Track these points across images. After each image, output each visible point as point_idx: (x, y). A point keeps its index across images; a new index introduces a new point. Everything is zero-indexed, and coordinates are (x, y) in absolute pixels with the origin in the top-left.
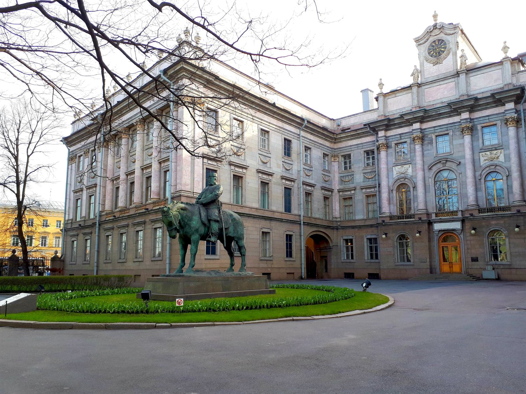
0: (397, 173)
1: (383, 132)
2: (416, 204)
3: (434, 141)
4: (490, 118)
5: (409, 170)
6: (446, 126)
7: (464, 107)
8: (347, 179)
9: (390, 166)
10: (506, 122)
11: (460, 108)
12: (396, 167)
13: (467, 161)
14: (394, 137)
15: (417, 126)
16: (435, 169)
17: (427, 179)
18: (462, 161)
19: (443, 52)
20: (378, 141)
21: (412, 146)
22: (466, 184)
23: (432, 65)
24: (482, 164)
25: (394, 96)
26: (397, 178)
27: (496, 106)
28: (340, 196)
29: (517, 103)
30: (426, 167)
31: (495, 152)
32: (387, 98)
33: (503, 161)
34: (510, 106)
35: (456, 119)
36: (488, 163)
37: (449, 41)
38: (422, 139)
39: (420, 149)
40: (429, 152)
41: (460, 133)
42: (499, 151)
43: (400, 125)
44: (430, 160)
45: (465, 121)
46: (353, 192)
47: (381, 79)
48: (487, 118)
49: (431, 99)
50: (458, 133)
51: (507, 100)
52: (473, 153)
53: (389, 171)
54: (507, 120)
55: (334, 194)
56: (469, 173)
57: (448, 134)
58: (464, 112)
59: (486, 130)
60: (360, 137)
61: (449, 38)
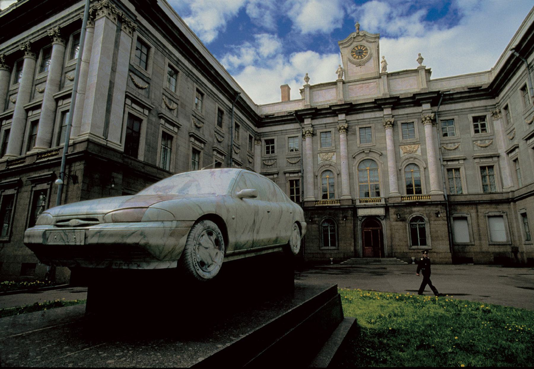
3: (358, 133)
15: (342, 117)
27: (414, 106)
30: (350, 155)
31: (413, 146)
33: (420, 154)
35: (378, 114)
36: (407, 156)
38: (347, 130)
42: (417, 146)
44: (355, 149)
53: (314, 157)
60: (285, 124)
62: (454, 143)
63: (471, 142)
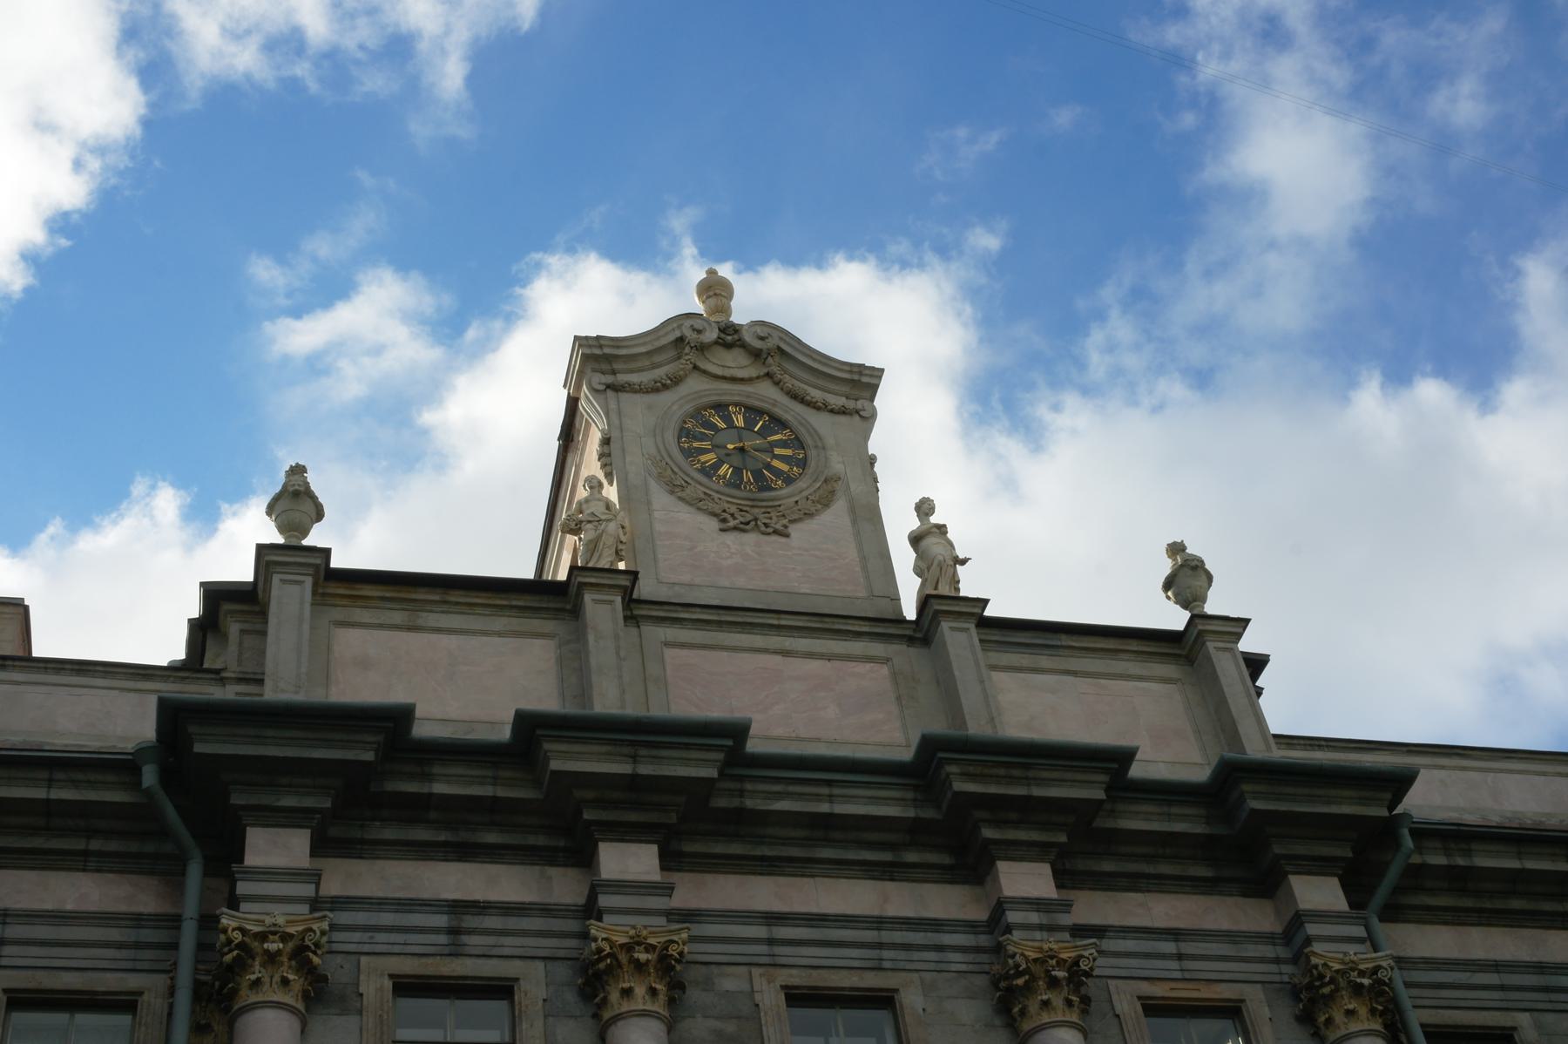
4: (1188, 948)
6: (870, 936)
11: (998, 807)
19: (789, 480)
23: (714, 524)
25: (398, 617)
32: (337, 614)
34: (1318, 893)
37: (815, 433)
43: (461, 832)
48: (1169, 947)
57: (884, 1000)
61: (821, 422)
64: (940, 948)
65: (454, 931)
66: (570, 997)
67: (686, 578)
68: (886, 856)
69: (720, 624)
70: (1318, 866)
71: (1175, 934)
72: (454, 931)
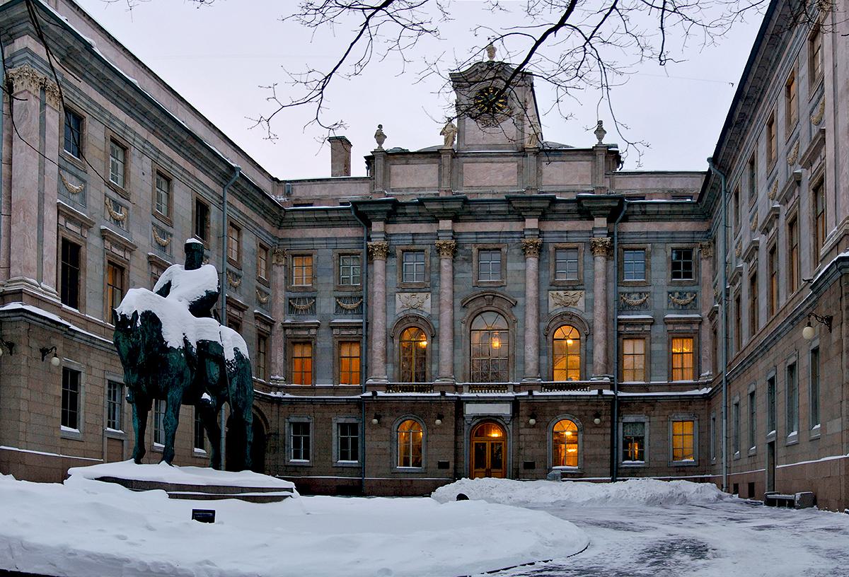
0: (403, 307)
1: (382, 223)
2: (434, 367)
3: (474, 259)
5: (425, 303)
6: (498, 236)
7: (532, 209)
8: (302, 306)
9: (392, 290)
10: (593, 247)
12: (403, 295)
13: (528, 301)
14: (401, 237)
15: (446, 224)
16: (473, 307)
17: (457, 324)
18: (520, 301)
20: (369, 239)
21: (434, 260)
22: (524, 340)
24: (551, 309)
26: (402, 315)
27: (580, 219)
28: (286, 337)
29: (611, 220)
30: (458, 302)
33: (583, 309)
34: (601, 222)
35: (516, 226)
38: (454, 251)
39: (450, 268)
40: (464, 275)
41: (520, 251)
42: (579, 292)
44: (466, 289)
45: (530, 233)
46: (313, 332)
47: (380, 126)
48: (565, 235)
49: (473, 183)
50: (516, 251)
51: (597, 212)
52: (539, 290)
54: (595, 244)
55: (274, 332)
56: (531, 323)
57: (500, 249)
58: (530, 217)
59: (560, 255)
60: (333, 226)
62: (640, 293)
63: (665, 294)
64: (513, 238)
65: (413, 240)
66: (435, 252)
67: (471, 143)
68: (504, 217)
69: (477, 157)
70: (603, 215)
71: (567, 232)
72: (413, 240)
